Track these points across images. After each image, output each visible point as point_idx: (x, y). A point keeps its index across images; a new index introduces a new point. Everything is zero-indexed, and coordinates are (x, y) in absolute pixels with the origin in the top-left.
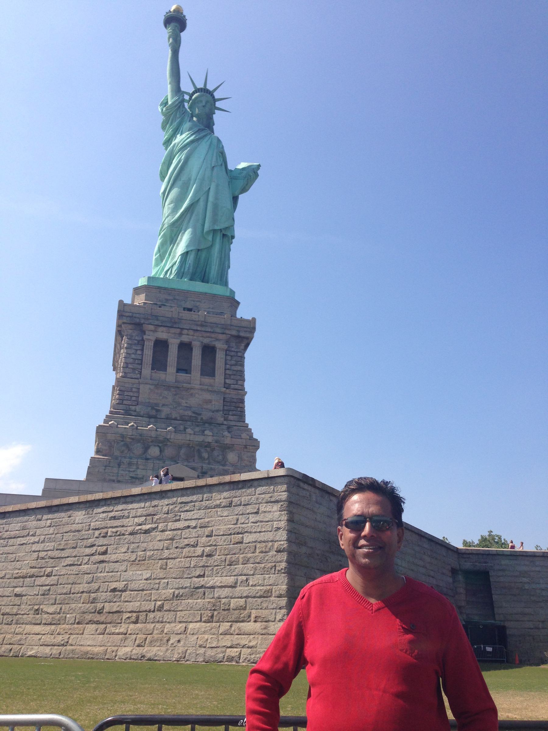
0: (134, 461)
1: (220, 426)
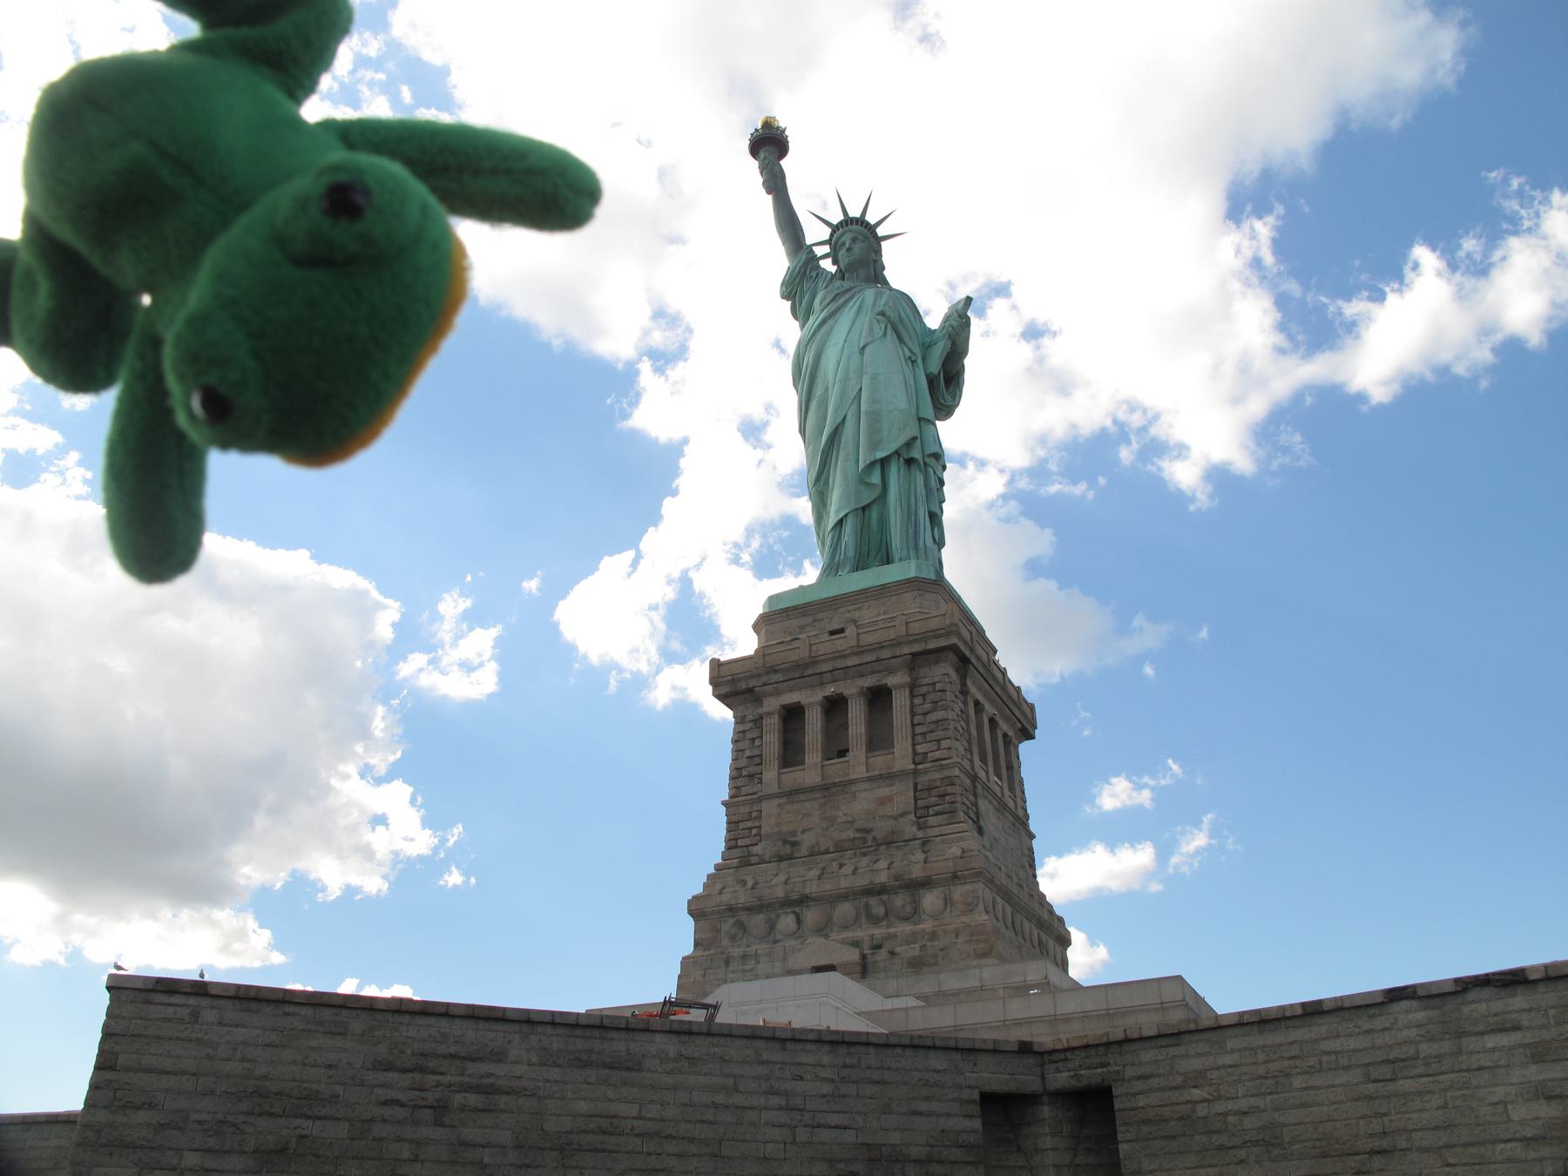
1: (906, 845)
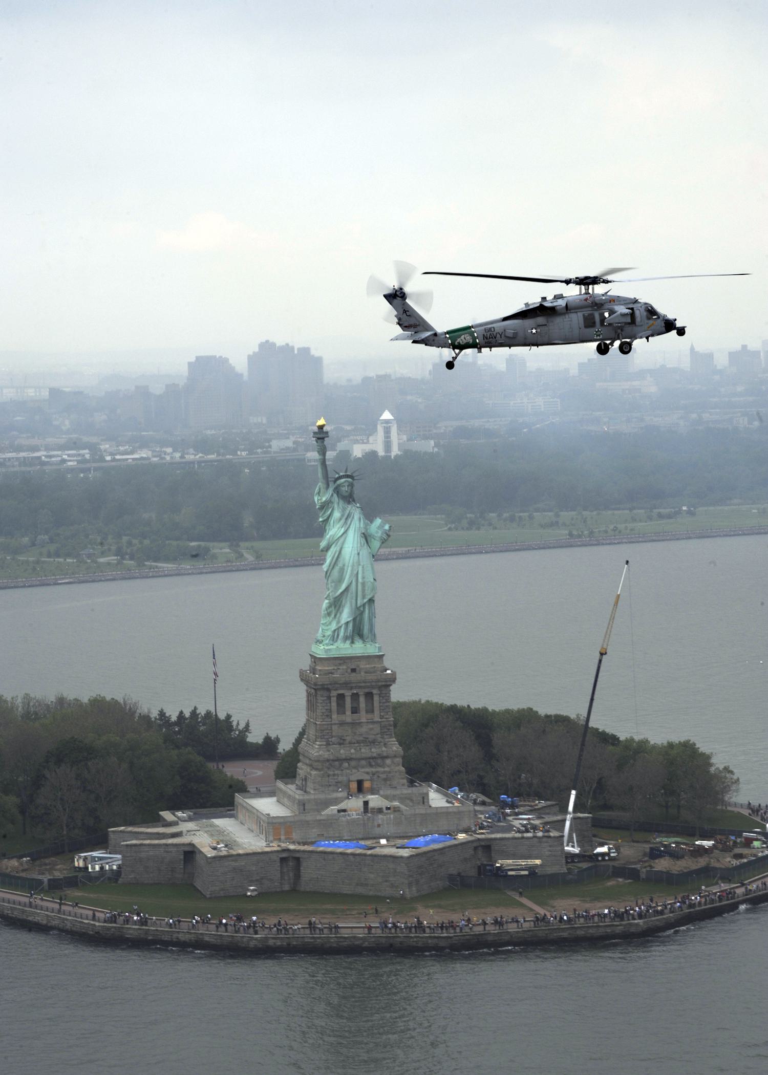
0: (336, 772)
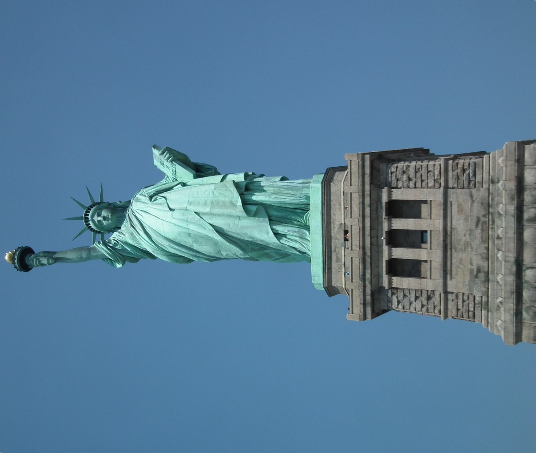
1: (492, 194)
